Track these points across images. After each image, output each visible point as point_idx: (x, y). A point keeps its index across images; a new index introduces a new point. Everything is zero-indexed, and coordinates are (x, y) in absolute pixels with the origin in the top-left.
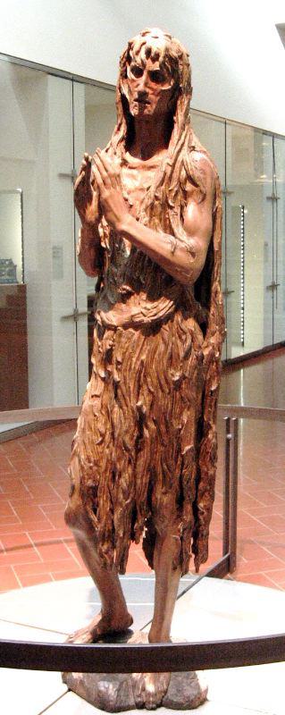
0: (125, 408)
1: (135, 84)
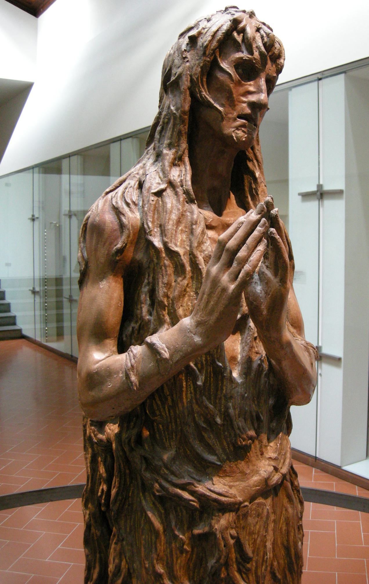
1: (241, 90)
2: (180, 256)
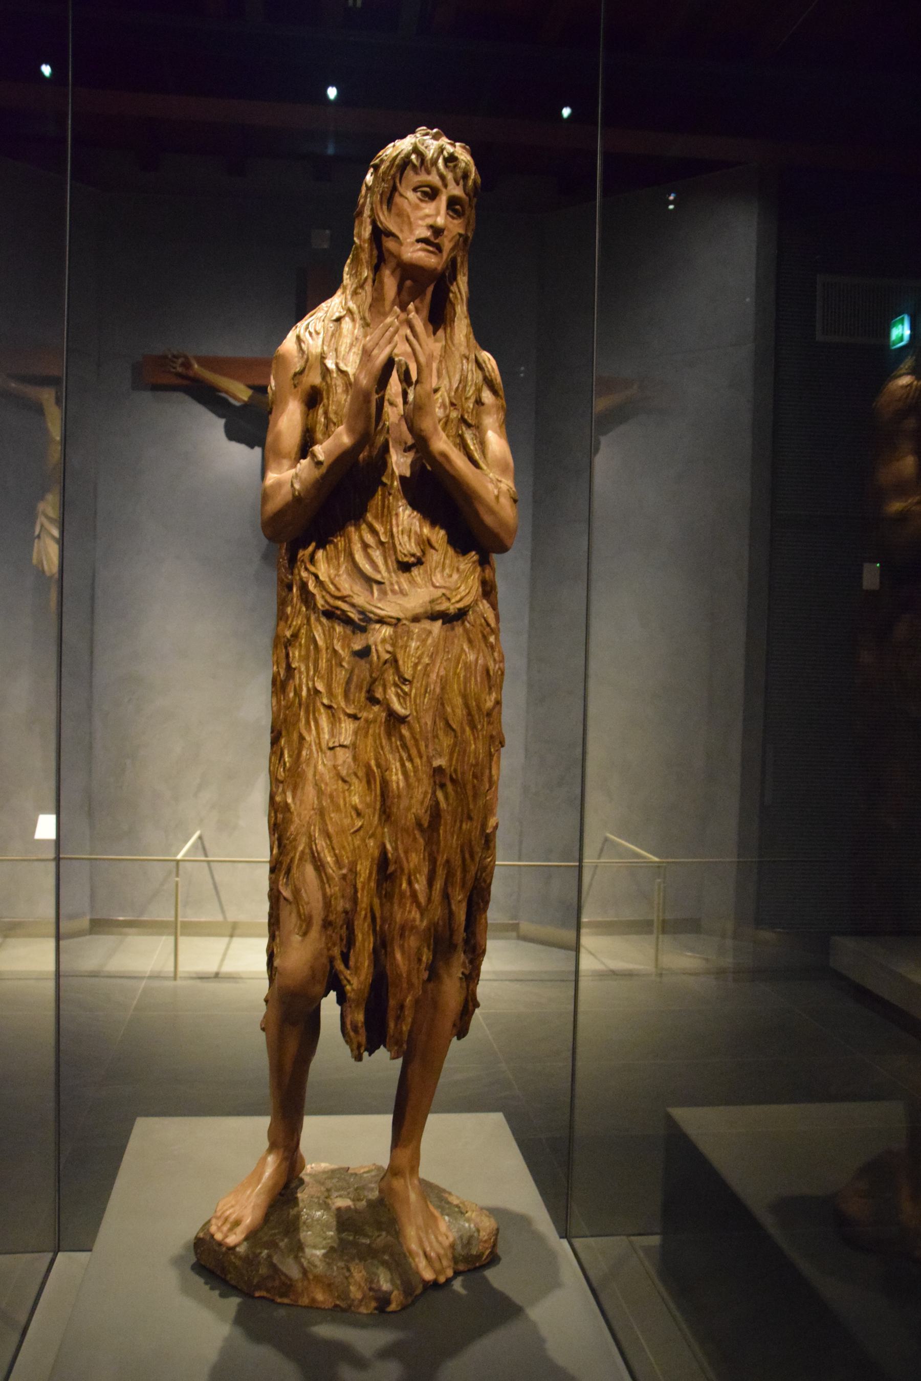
0: (417, 761)
1: (421, 214)
2: (349, 375)
